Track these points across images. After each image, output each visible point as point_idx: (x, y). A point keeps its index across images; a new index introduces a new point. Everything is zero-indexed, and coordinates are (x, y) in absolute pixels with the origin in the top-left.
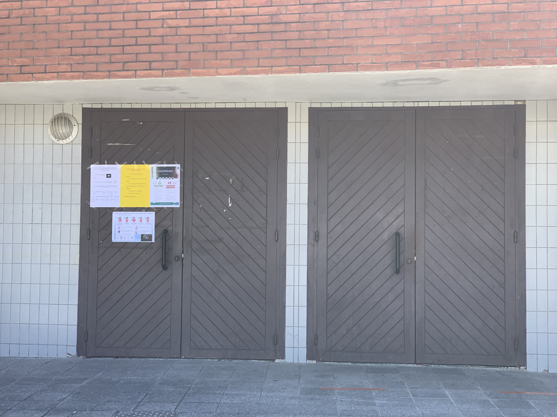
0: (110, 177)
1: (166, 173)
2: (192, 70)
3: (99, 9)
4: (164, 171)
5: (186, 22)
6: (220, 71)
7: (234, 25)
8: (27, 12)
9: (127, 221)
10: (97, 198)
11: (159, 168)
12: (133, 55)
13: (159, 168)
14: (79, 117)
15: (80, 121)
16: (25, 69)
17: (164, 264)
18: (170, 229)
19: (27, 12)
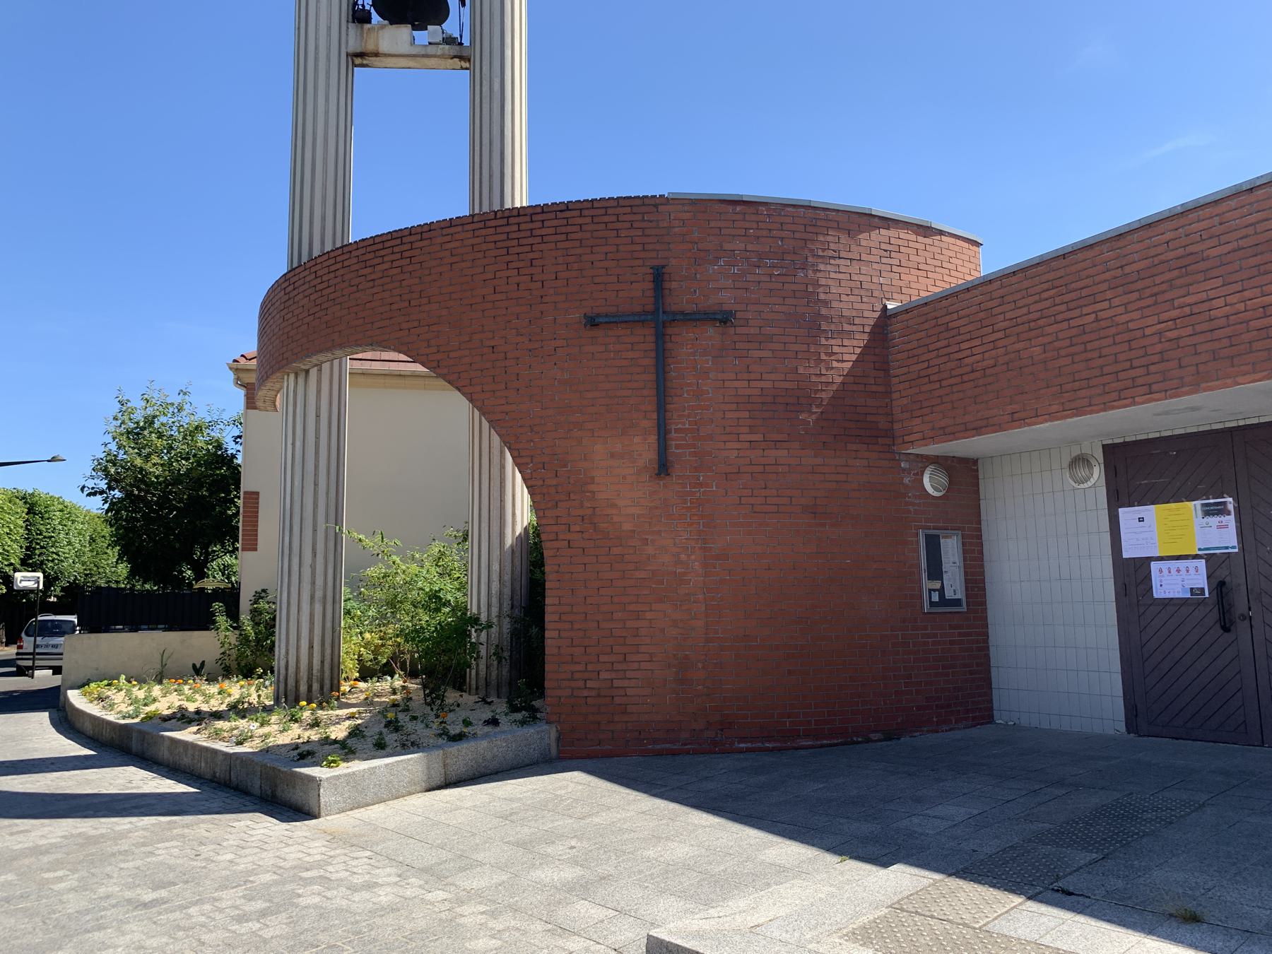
0: (1143, 521)
1: (1215, 510)
2: (1203, 385)
3: (1085, 338)
4: (1212, 508)
5: (1189, 330)
6: (1239, 379)
7: (1251, 321)
8: (1012, 356)
9: (1170, 572)
10: (1131, 547)
11: (1203, 505)
12: (1129, 381)
13: (1203, 505)
14: (1099, 455)
15: (1101, 460)
16: (1016, 416)
17: (1222, 624)
18: (1228, 580)
19: (1012, 356)
